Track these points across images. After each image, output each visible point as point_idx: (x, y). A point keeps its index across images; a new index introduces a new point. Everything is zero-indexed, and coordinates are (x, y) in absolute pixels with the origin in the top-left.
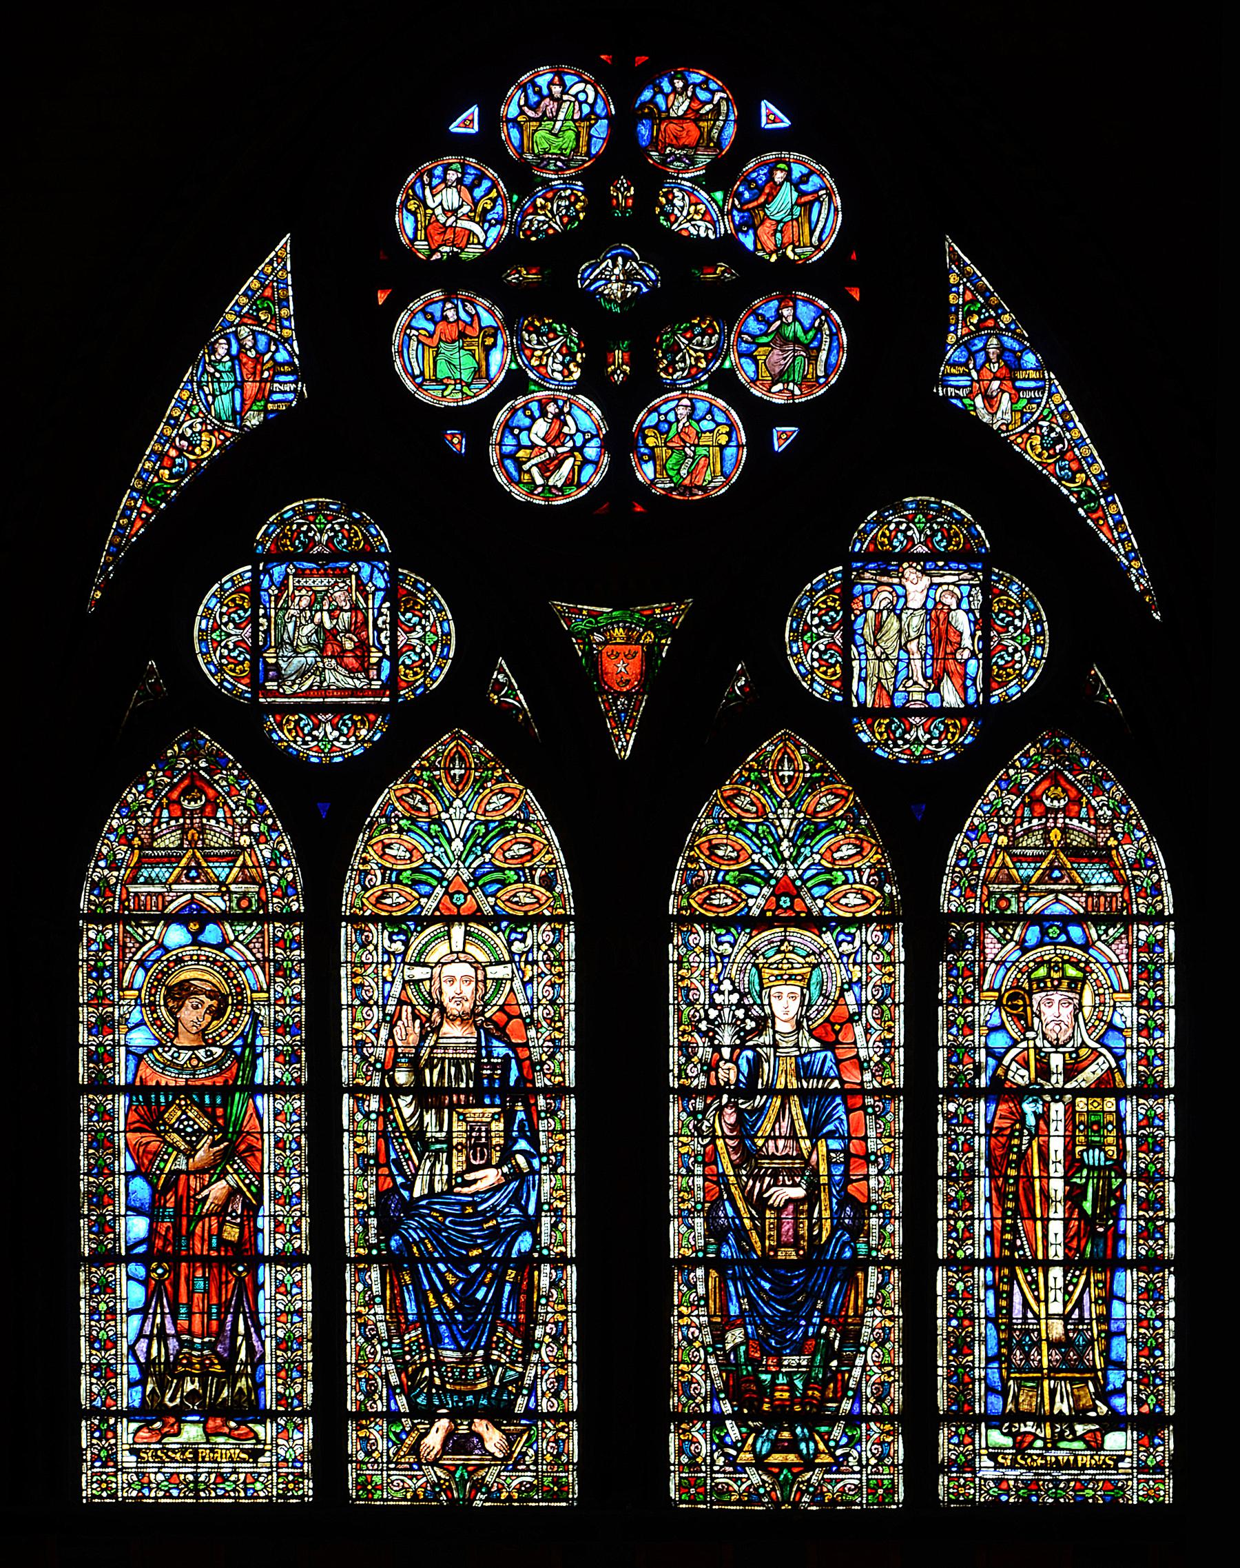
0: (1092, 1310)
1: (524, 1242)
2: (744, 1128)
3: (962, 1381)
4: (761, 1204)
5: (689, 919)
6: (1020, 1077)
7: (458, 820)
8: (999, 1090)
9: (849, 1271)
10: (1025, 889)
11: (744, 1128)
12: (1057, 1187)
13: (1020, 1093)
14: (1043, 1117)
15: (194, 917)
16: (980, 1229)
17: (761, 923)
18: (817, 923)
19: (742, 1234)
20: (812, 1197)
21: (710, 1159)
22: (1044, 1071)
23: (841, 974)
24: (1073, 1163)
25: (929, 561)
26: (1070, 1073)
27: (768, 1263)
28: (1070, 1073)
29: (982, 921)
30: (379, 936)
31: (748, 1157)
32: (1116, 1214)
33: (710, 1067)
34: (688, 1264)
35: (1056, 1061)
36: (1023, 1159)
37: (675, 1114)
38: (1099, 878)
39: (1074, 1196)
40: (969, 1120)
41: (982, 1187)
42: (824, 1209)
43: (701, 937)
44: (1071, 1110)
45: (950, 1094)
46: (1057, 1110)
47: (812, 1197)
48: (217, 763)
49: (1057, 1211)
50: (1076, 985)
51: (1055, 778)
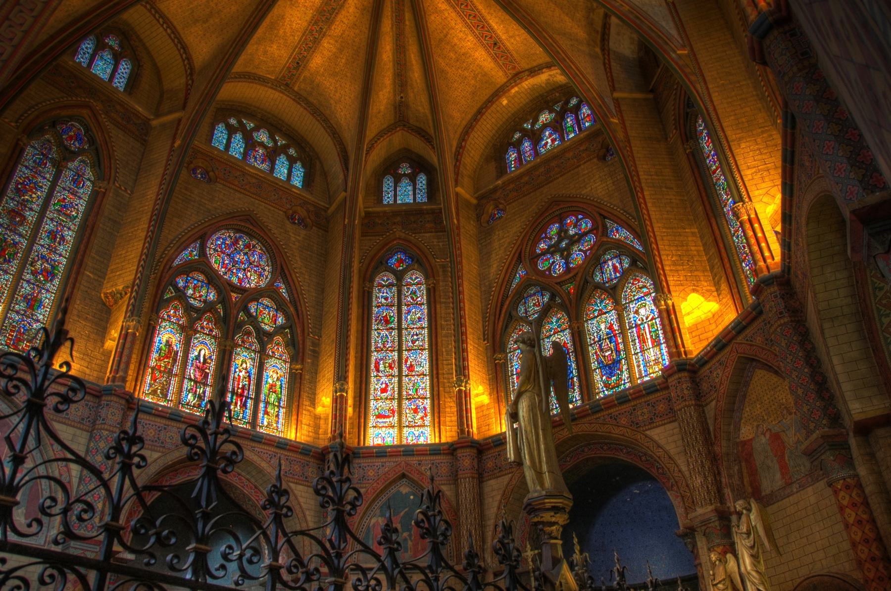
0: (658, 353)
1: (571, 375)
2: (600, 346)
3: (640, 371)
4: (604, 357)
5: (587, 321)
6: (639, 322)
7: (554, 319)
8: (637, 326)
9: (619, 361)
10: (634, 296)
11: (600, 346)
12: (649, 337)
13: (640, 325)
14: (644, 327)
16: (638, 348)
17: (598, 316)
18: (605, 313)
19: (602, 362)
20: (612, 353)
21: (596, 353)
22: (643, 320)
23: (610, 319)
24: (650, 332)
25: (611, 259)
26: (647, 319)
27: (607, 365)
28: (647, 319)
29: (629, 303)
30: (546, 340)
31: (601, 350)
32: (659, 337)
33: (594, 340)
34: (595, 369)
35: (644, 318)
36: (643, 334)
37: (590, 348)
38: (645, 290)
39: (651, 337)
40: (633, 332)
41: (637, 341)
42: (614, 354)
43: (590, 322)
44: (648, 325)
45: (629, 329)
46: (646, 325)
47: (612, 353)
48: (523, 326)
49: (649, 340)
50: (645, 306)
51: (636, 279)
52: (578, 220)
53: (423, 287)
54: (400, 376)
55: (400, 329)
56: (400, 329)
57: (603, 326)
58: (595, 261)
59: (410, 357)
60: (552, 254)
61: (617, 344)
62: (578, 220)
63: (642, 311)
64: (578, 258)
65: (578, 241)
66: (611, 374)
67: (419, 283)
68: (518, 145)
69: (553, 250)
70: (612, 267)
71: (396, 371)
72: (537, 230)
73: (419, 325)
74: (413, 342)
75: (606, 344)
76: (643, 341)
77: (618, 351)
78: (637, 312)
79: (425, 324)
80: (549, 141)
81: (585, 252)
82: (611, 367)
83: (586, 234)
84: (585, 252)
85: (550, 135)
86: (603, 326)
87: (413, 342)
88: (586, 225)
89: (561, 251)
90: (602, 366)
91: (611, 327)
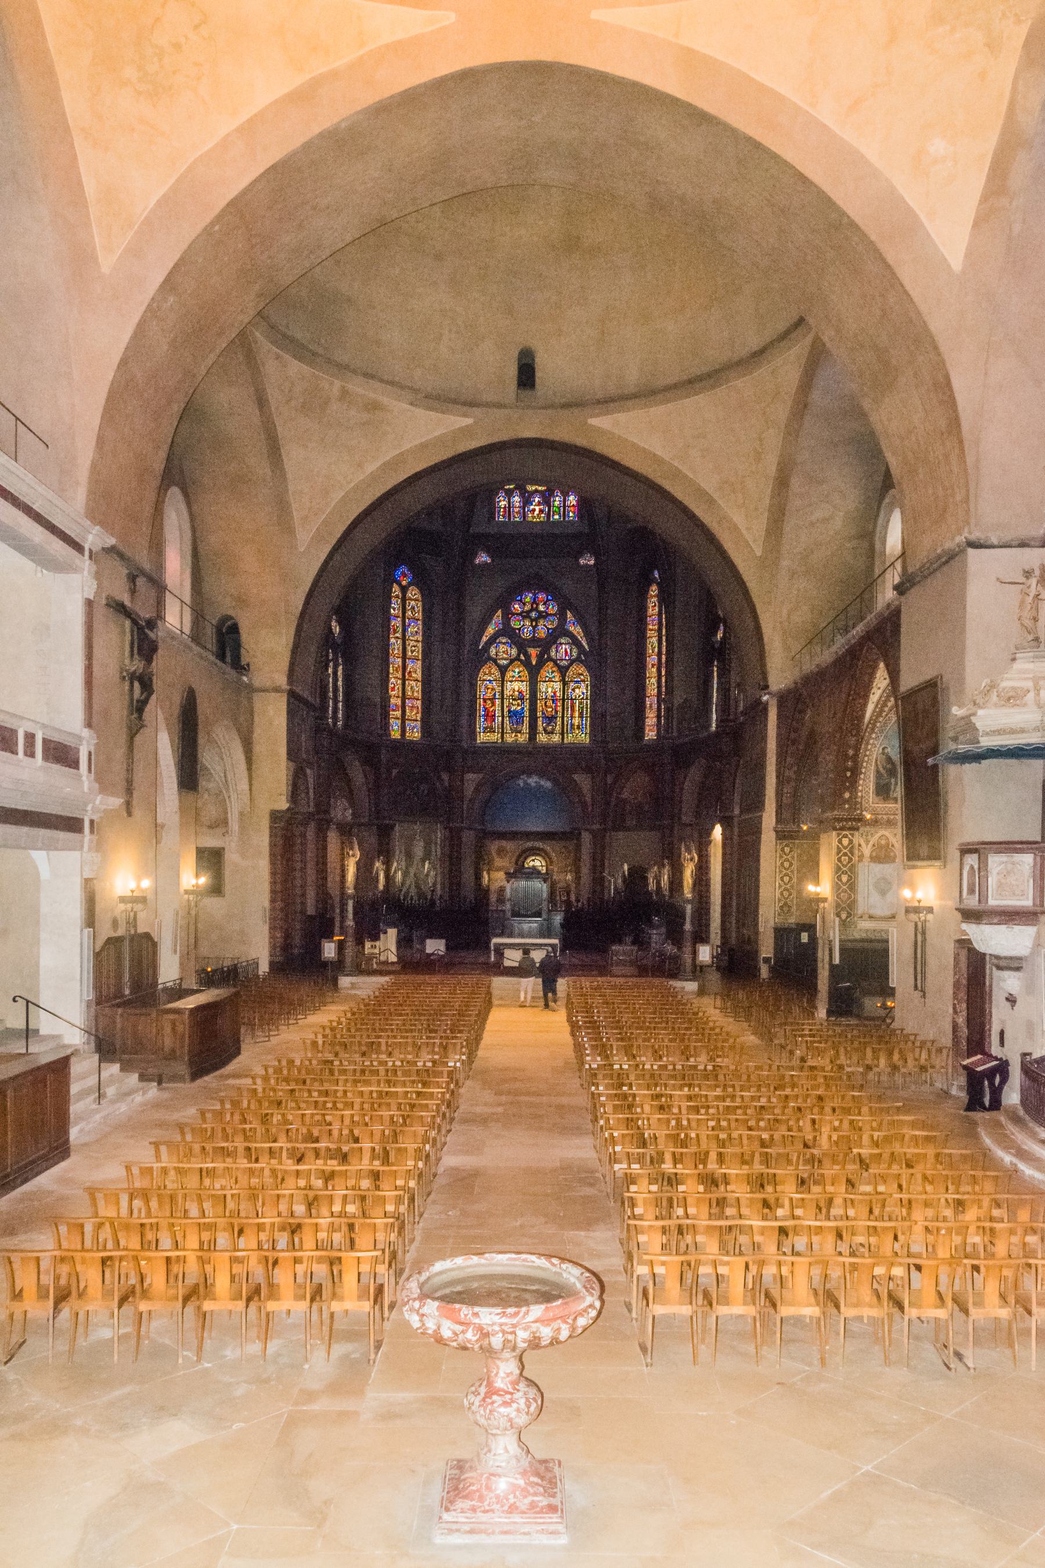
7: (517, 670)
15: (490, 681)
52: (548, 600)
53: (420, 604)
54: (404, 680)
55: (404, 639)
56: (404, 639)
57: (550, 690)
58: (553, 638)
59: (410, 666)
60: (524, 617)
61: (556, 706)
62: (548, 600)
63: (577, 690)
64: (542, 633)
65: (545, 617)
66: (548, 725)
67: (416, 600)
68: (509, 494)
69: (525, 615)
70: (563, 650)
71: (400, 675)
72: (513, 593)
73: (415, 638)
74: (412, 652)
75: (550, 703)
76: (573, 710)
77: (556, 712)
78: (573, 690)
79: (420, 638)
80: (537, 508)
81: (548, 629)
82: (551, 719)
83: (551, 615)
84: (548, 629)
85: (539, 504)
86: (550, 690)
87: (412, 652)
88: (553, 608)
89: (532, 621)
90: (545, 717)
91: (555, 693)
